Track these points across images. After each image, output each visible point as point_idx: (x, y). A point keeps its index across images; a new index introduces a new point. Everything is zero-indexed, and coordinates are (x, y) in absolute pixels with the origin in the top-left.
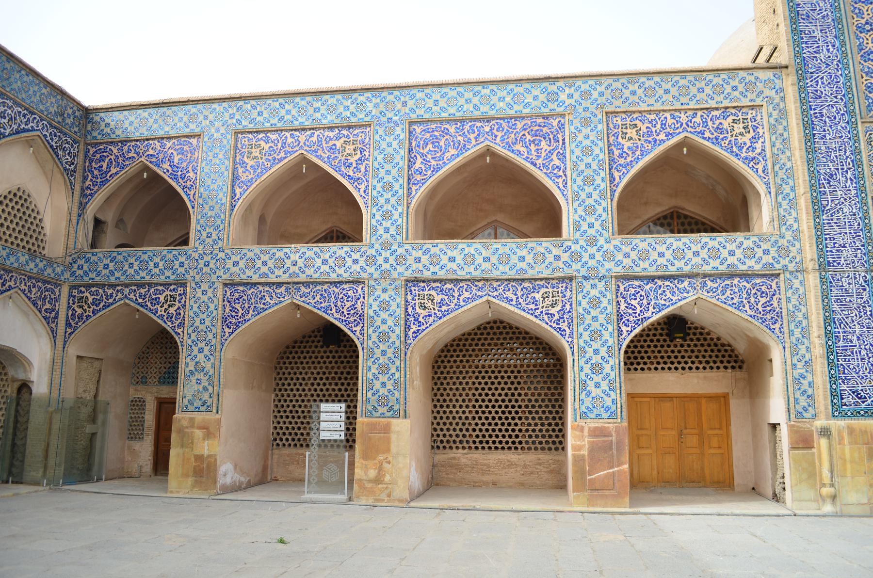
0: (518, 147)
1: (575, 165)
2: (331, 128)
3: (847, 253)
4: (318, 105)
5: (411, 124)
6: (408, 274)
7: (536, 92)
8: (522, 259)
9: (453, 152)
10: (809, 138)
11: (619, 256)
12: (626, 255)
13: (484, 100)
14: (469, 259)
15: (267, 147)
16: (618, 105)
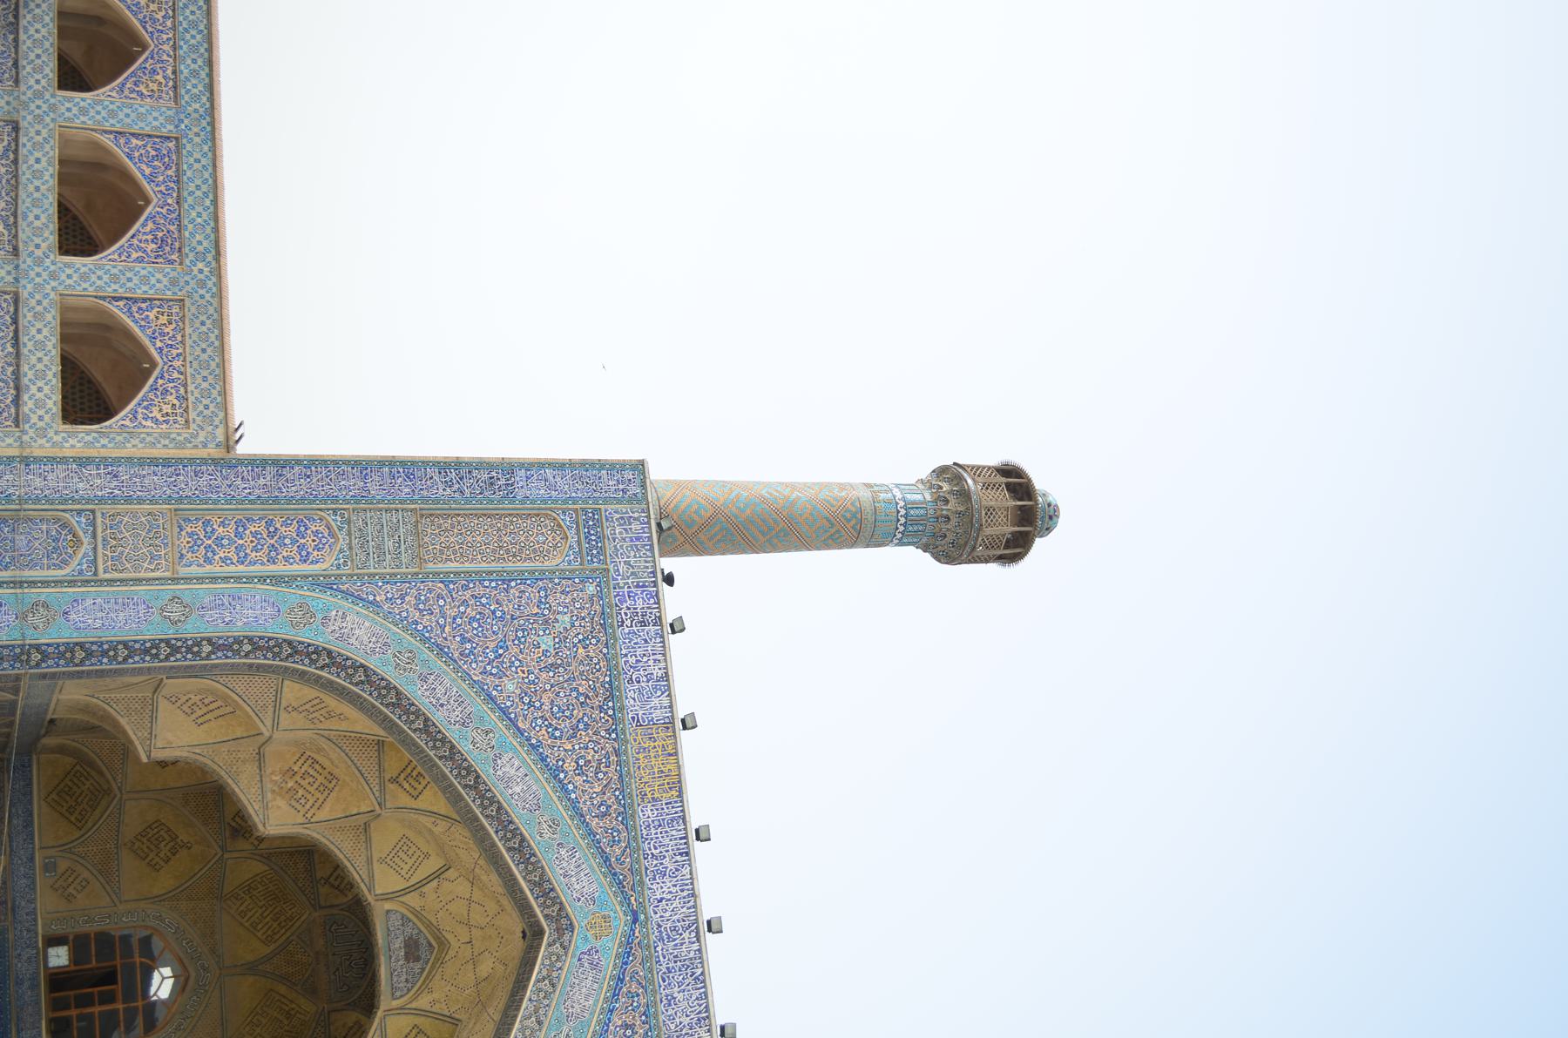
0: (150, 225)
1: (130, 270)
2: (174, 72)
3: (38, 482)
4: (200, 62)
5: (177, 139)
6: (23, 124)
7: (205, 244)
8: (37, 218)
9: (147, 171)
10: (154, 462)
11: (38, 297)
12: (39, 303)
13: (199, 201)
14: (37, 175)
15: (159, 16)
16: (191, 310)
